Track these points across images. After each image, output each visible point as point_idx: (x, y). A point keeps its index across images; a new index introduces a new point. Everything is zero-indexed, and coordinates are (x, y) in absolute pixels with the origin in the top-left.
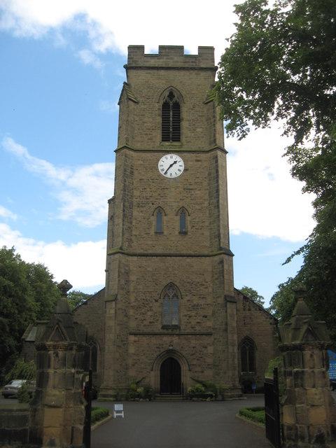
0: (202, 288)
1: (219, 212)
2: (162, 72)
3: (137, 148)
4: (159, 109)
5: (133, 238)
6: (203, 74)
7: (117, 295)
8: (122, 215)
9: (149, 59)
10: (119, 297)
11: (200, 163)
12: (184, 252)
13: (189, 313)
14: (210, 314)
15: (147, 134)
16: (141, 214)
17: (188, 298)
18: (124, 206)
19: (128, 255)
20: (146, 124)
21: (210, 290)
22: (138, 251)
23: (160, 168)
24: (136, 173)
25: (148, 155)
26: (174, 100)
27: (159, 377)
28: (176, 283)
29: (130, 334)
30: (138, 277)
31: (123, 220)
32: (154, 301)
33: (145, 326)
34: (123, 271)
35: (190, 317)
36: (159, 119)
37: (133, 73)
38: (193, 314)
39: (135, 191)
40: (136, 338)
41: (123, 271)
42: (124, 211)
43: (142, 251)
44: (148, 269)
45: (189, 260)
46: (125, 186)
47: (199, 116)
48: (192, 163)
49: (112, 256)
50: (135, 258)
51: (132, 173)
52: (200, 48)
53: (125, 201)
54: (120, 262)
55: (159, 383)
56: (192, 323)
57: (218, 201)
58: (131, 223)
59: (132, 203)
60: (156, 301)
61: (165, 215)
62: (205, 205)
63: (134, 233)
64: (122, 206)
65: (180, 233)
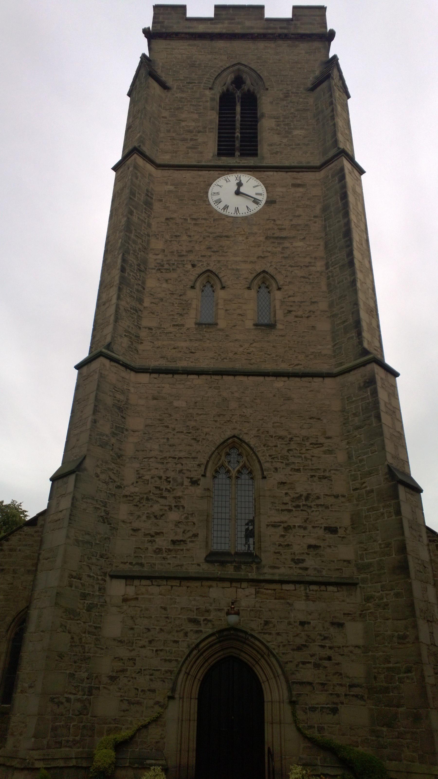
0: (316, 451)
1: (354, 273)
2: (221, 44)
3: (162, 162)
4: (212, 99)
5: (143, 334)
6: (303, 46)
7: (84, 458)
8: (117, 278)
9: (195, 24)
10: (88, 464)
11: (301, 190)
12: (269, 367)
13: (284, 517)
14: (346, 521)
15: (184, 140)
16: (165, 285)
17: (279, 477)
18: (124, 260)
19: (126, 366)
20: (183, 124)
21: (341, 457)
22: (153, 364)
23: (212, 199)
24: (157, 206)
25: (188, 175)
26: (245, 88)
27: (194, 725)
28: (246, 438)
29: (112, 577)
30: (149, 422)
31: (120, 289)
32: (186, 482)
33: (158, 551)
34: (109, 401)
35: (287, 529)
36: (214, 116)
37: (161, 44)
38: (298, 522)
39: (153, 240)
40: (131, 591)
41: (109, 401)
42: (123, 270)
43: (162, 363)
44: (176, 404)
45: (279, 383)
46: (129, 223)
47: (298, 110)
48: (284, 190)
49: (85, 369)
50: (144, 378)
51: (148, 204)
52: (295, 8)
53: (126, 252)
54: (101, 376)
55: (193, 745)
56: (296, 549)
57: (350, 254)
58: (141, 301)
59: (145, 262)
60: (194, 482)
61: (223, 288)
62: (319, 269)
63: (145, 323)
64: (119, 261)
65: (255, 325)
